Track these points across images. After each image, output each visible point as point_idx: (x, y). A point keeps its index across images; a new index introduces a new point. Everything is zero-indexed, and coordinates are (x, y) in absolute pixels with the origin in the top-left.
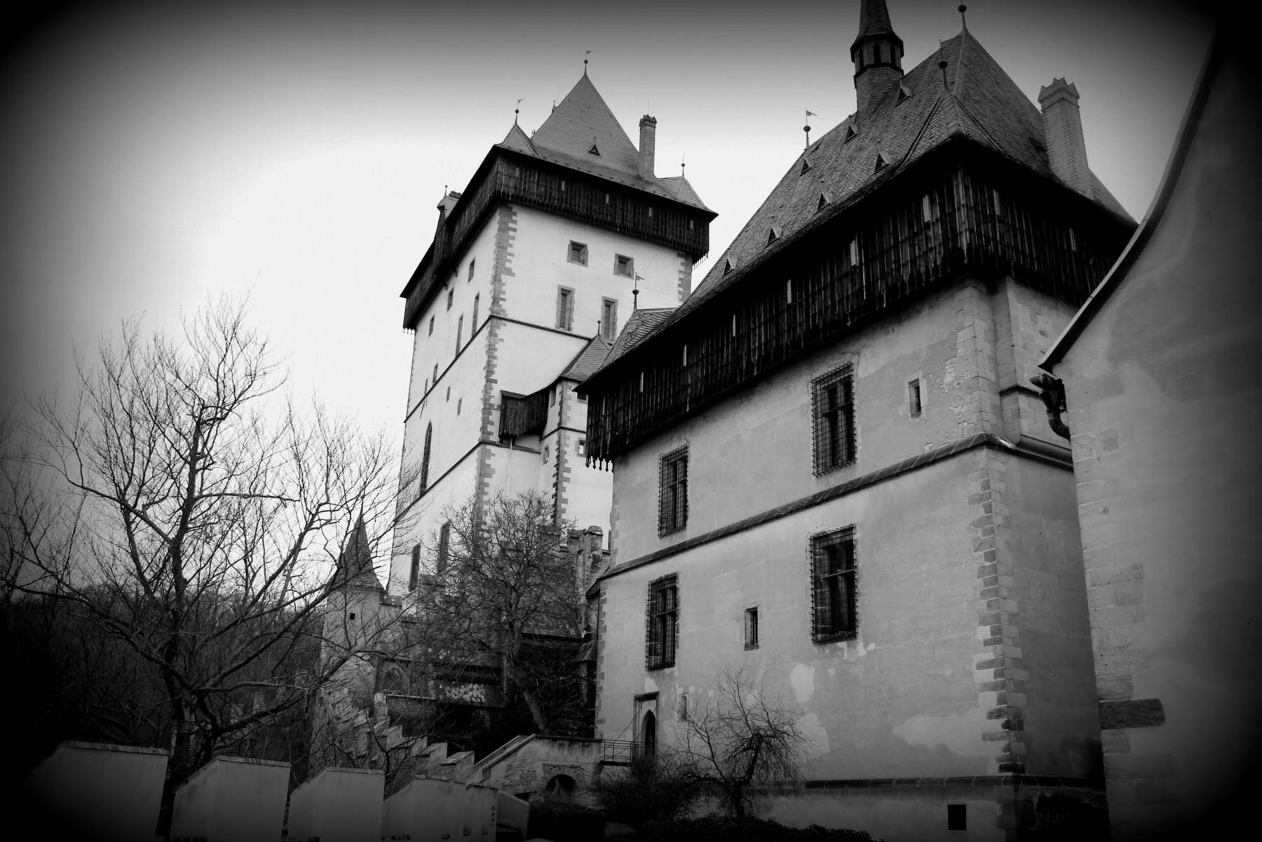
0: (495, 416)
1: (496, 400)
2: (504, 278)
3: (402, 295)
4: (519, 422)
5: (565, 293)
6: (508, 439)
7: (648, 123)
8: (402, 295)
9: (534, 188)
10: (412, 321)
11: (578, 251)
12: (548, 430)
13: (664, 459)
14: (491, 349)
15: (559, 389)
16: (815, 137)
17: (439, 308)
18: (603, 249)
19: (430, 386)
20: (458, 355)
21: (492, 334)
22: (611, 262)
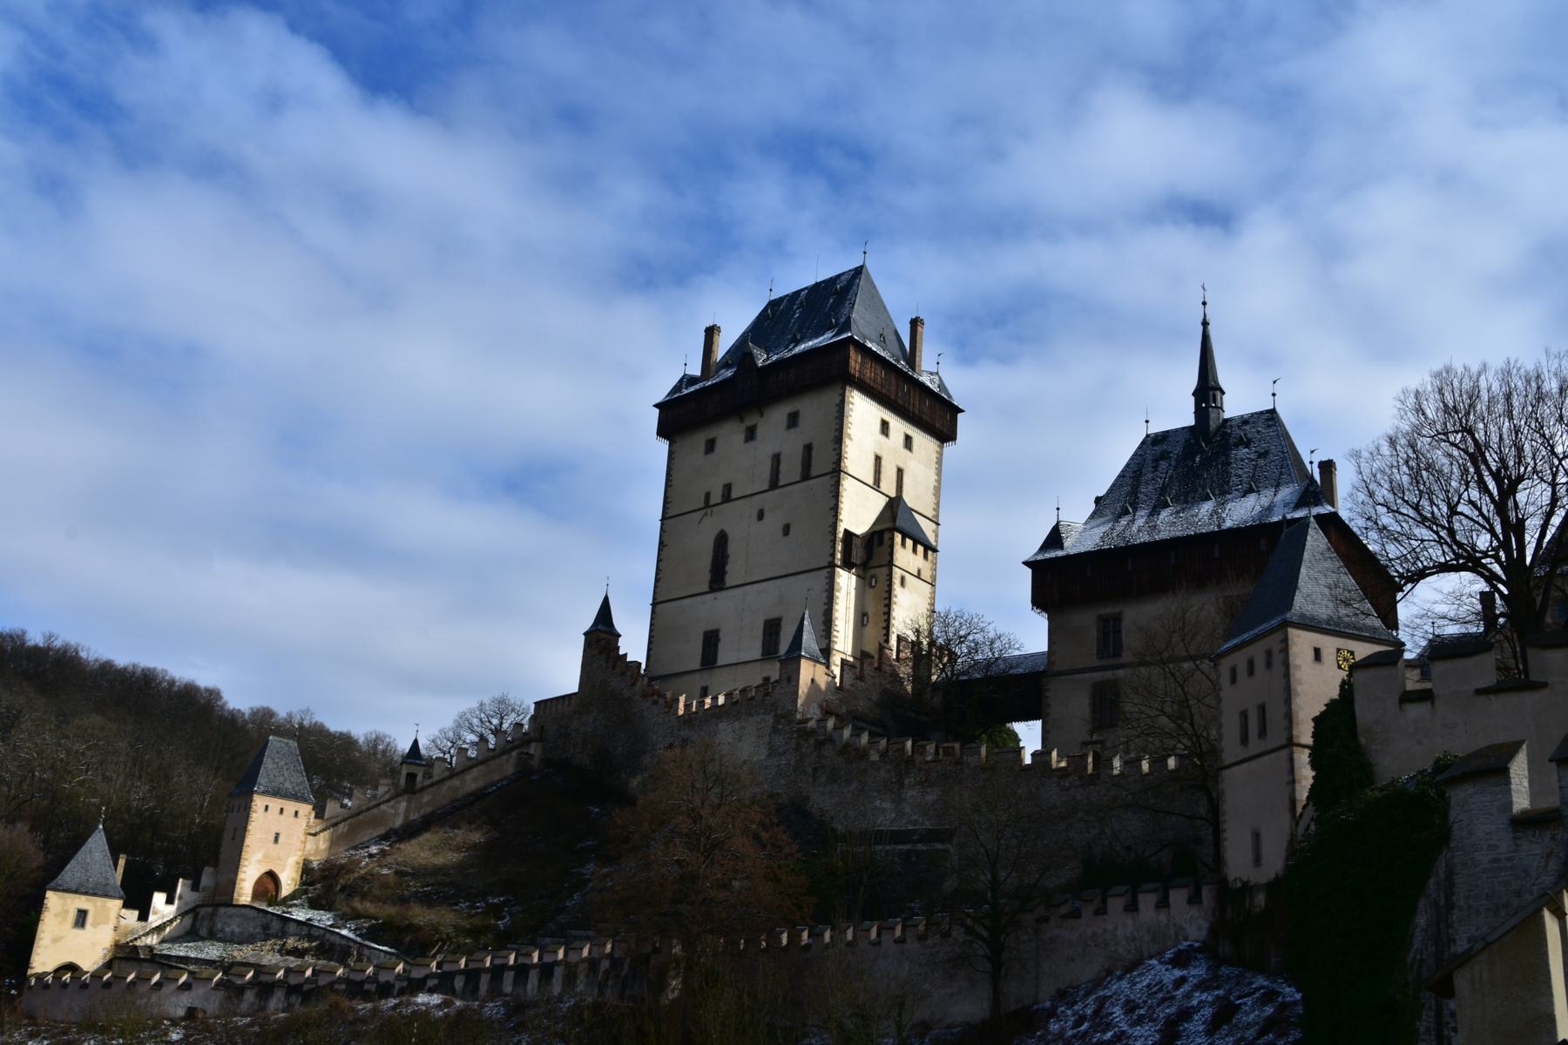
0: (839, 547)
1: (840, 535)
2: (847, 441)
3: (656, 406)
4: (858, 555)
5: (878, 459)
6: (848, 565)
7: (915, 323)
8: (656, 406)
9: (871, 373)
10: (666, 429)
11: (885, 426)
12: (874, 562)
13: (1100, 617)
14: (836, 495)
15: (887, 536)
16: (1157, 427)
17: (729, 435)
18: (899, 427)
19: (716, 498)
20: (774, 484)
21: (837, 484)
22: (901, 439)
